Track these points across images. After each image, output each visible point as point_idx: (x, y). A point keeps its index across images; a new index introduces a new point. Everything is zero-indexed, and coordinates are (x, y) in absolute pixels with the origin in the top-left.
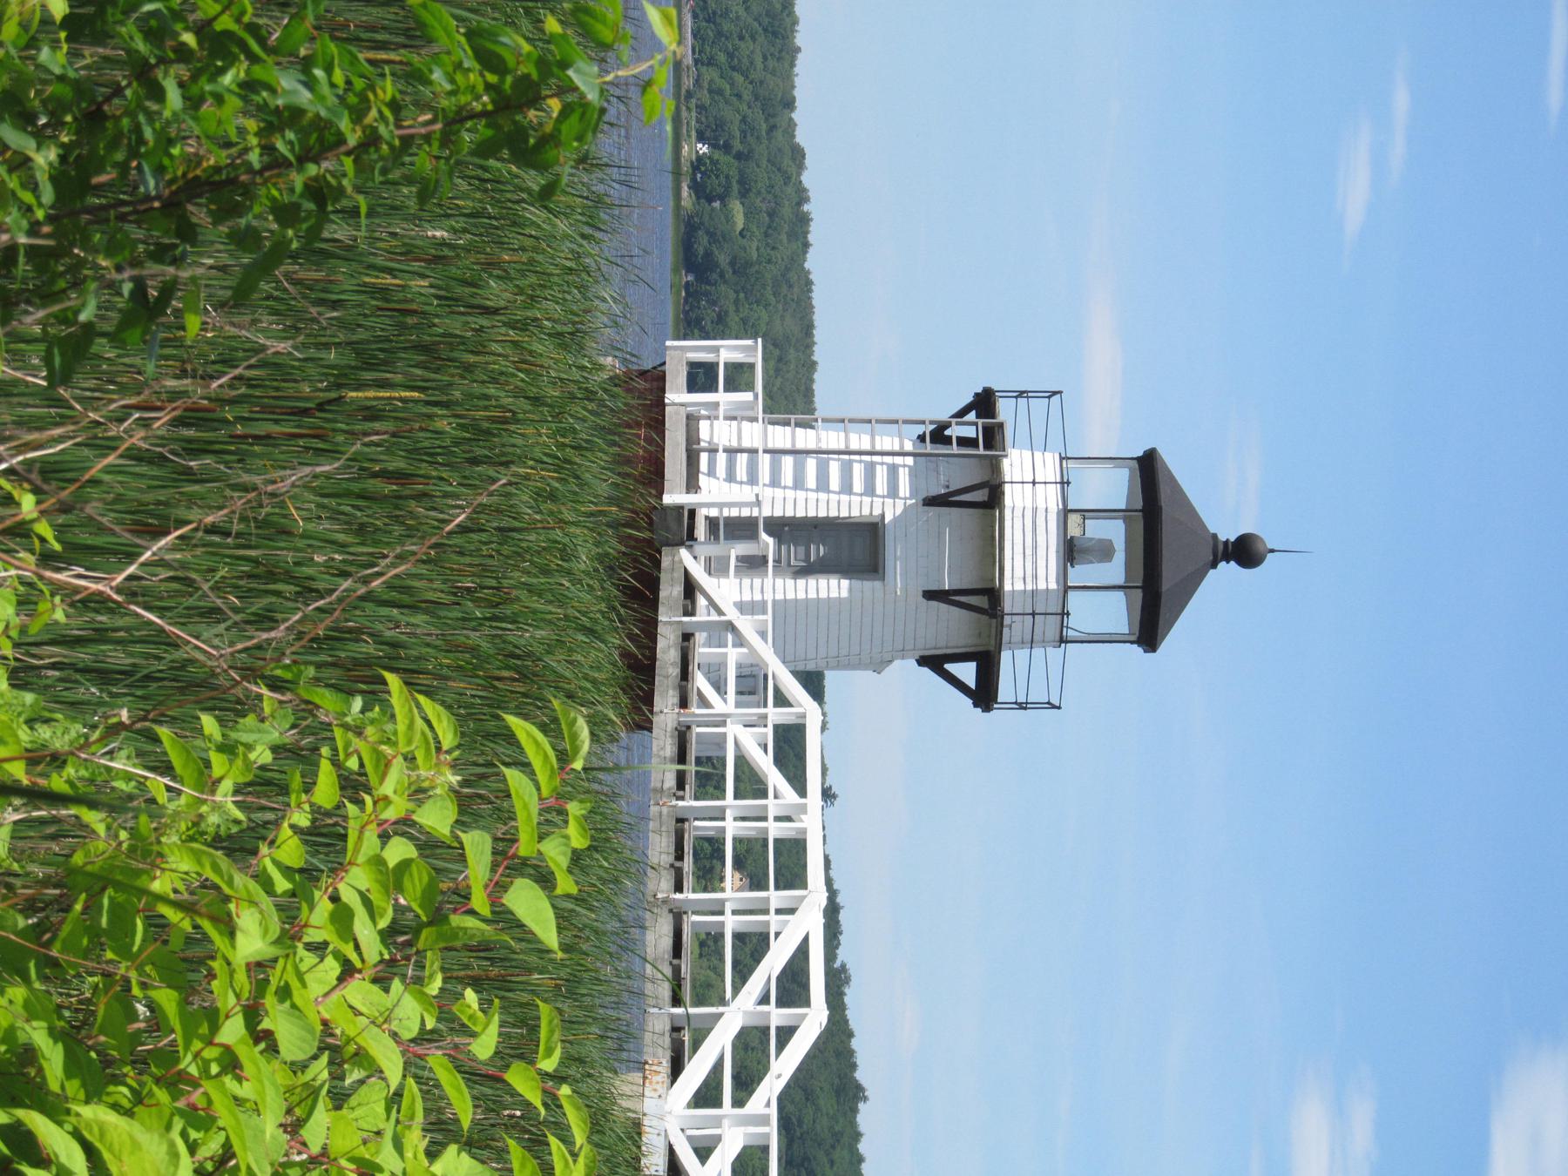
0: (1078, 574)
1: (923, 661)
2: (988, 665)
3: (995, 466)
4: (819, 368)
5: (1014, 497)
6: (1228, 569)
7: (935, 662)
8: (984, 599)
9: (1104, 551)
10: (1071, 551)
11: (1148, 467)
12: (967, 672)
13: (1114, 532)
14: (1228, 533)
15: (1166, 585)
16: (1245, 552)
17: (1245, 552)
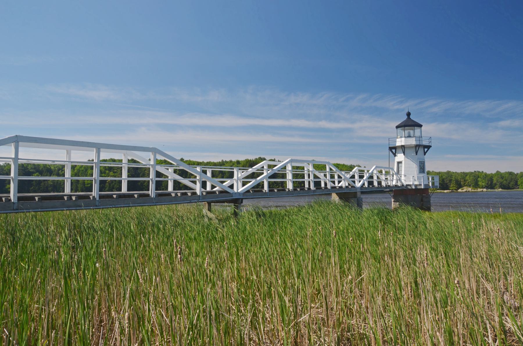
0: (412, 135)
1: (425, 155)
2: (425, 147)
3: (399, 146)
4: (449, 170)
5: (403, 144)
6: (411, 117)
7: (425, 153)
8: (417, 147)
9: (409, 133)
10: (409, 136)
11: (397, 127)
12: (426, 150)
13: (407, 132)
14: (406, 117)
15: (413, 124)
16: (409, 114)
17: (409, 114)
